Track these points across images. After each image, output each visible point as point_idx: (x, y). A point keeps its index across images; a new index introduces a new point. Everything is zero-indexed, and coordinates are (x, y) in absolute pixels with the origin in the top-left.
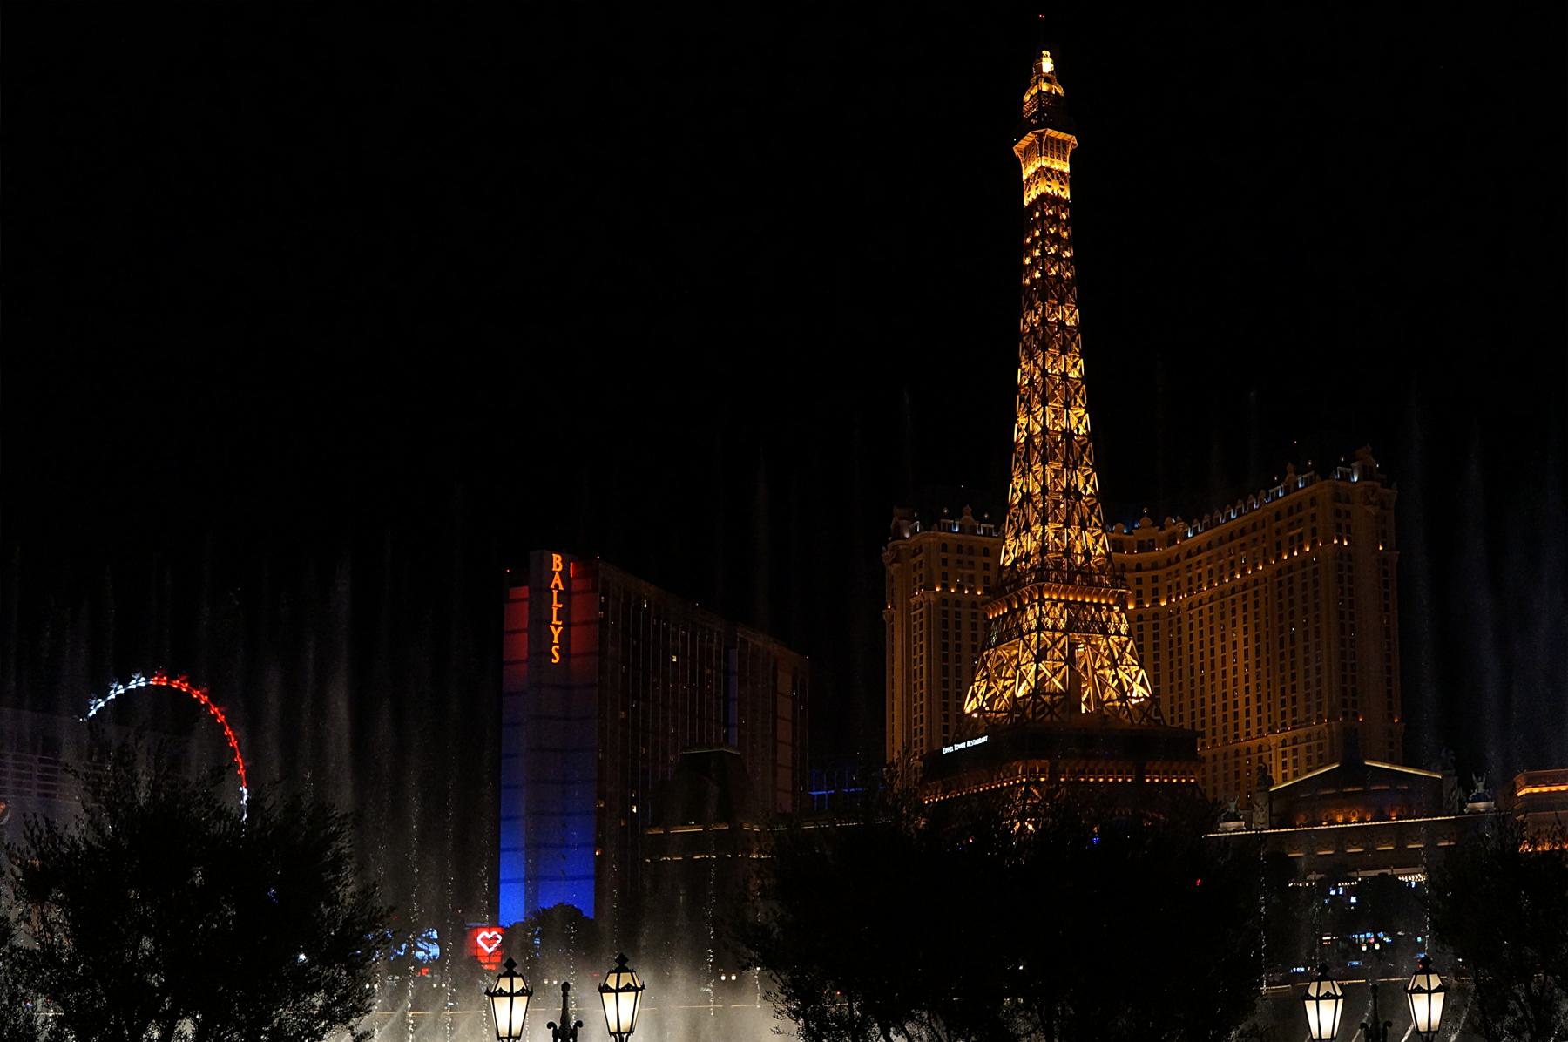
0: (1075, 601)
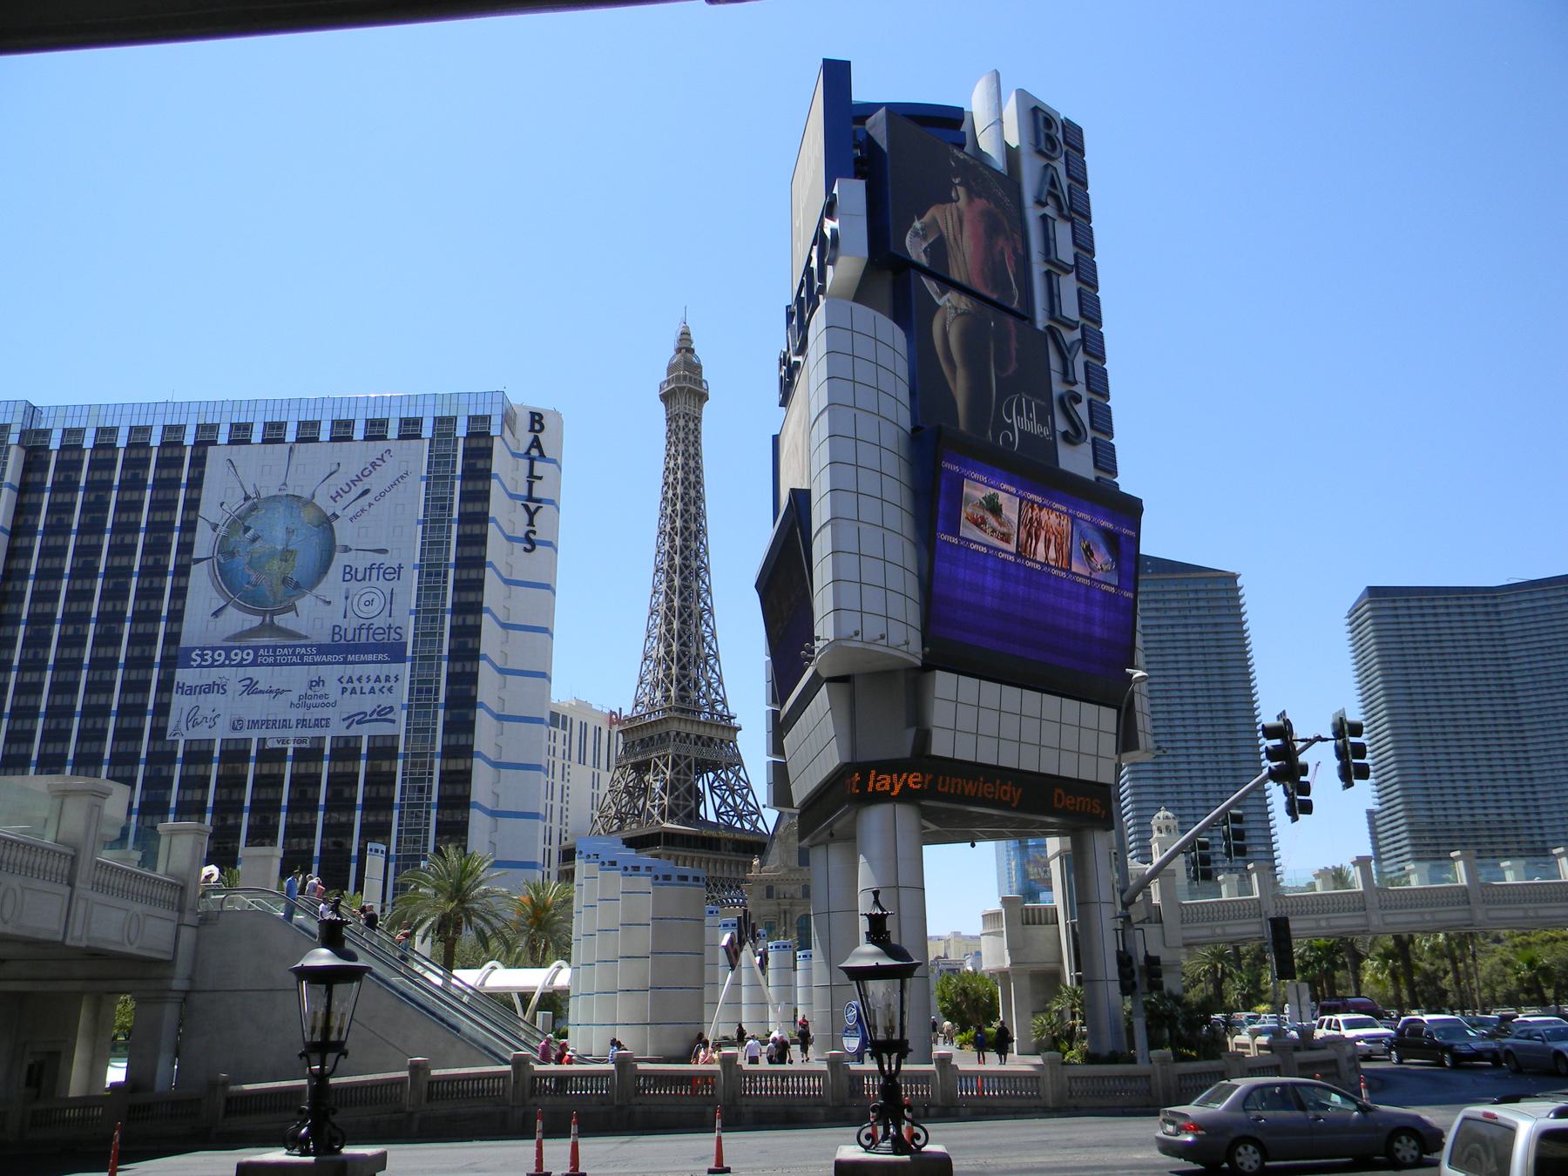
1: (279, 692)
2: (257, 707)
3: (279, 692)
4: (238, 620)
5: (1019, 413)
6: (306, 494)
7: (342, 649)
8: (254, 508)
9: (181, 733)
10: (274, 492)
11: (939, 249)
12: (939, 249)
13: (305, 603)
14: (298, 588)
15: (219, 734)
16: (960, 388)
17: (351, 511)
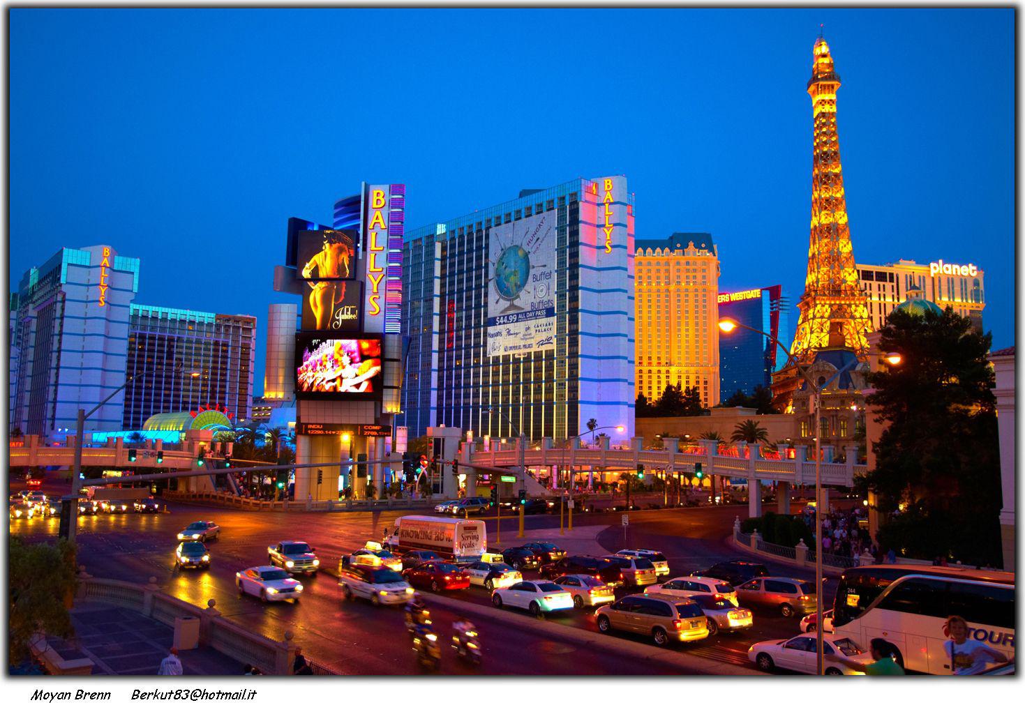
0: (835, 304)
1: (517, 334)
2: (511, 341)
3: (517, 334)
4: (504, 304)
5: (343, 313)
6: (519, 245)
7: (533, 313)
8: (504, 254)
9: (491, 354)
10: (510, 245)
11: (316, 270)
12: (316, 270)
13: (522, 293)
14: (520, 287)
15: (501, 353)
16: (318, 314)
17: (533, 250)
